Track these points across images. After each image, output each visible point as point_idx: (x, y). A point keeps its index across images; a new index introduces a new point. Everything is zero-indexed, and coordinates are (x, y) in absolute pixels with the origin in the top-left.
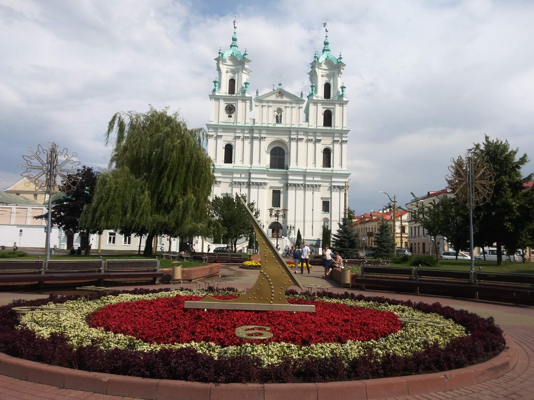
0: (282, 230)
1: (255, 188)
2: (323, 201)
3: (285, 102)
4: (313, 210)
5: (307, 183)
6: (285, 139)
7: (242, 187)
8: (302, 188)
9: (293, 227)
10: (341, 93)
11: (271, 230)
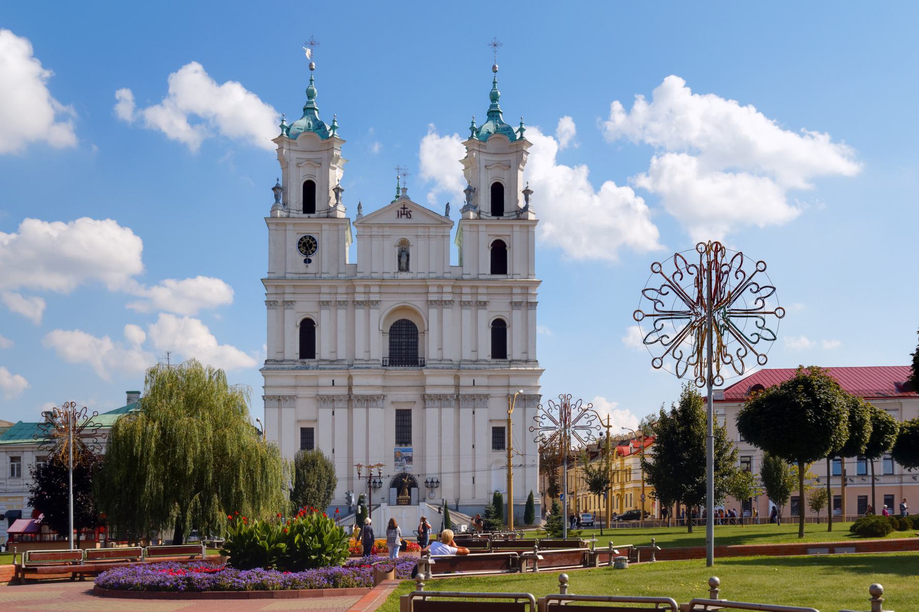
0: (416, 489)
1: (362, 407)
2: (494, 428)
3: (416, 226)
4: (473, 446)
6: (417, 302)
7: (336, 406)
8: (453, 402)
9: (437, 482)
10: (522, 204)
11: (395, 490)
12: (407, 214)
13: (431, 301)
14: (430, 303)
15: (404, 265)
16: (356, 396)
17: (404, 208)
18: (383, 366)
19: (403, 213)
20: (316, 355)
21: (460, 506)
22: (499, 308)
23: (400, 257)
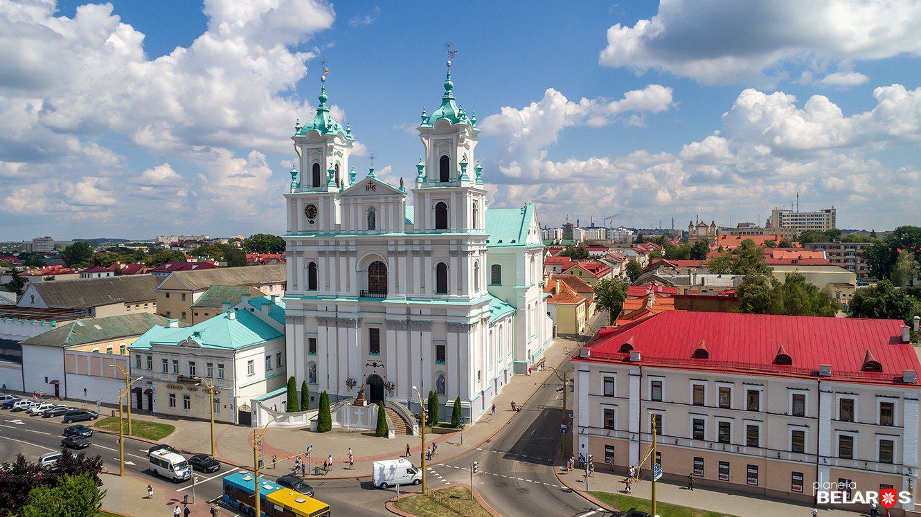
5: (413, 318)
13: (390, 252)
14: (391, 253)
16: (340, 319)
17: (371, 183)
22: (440, 255)
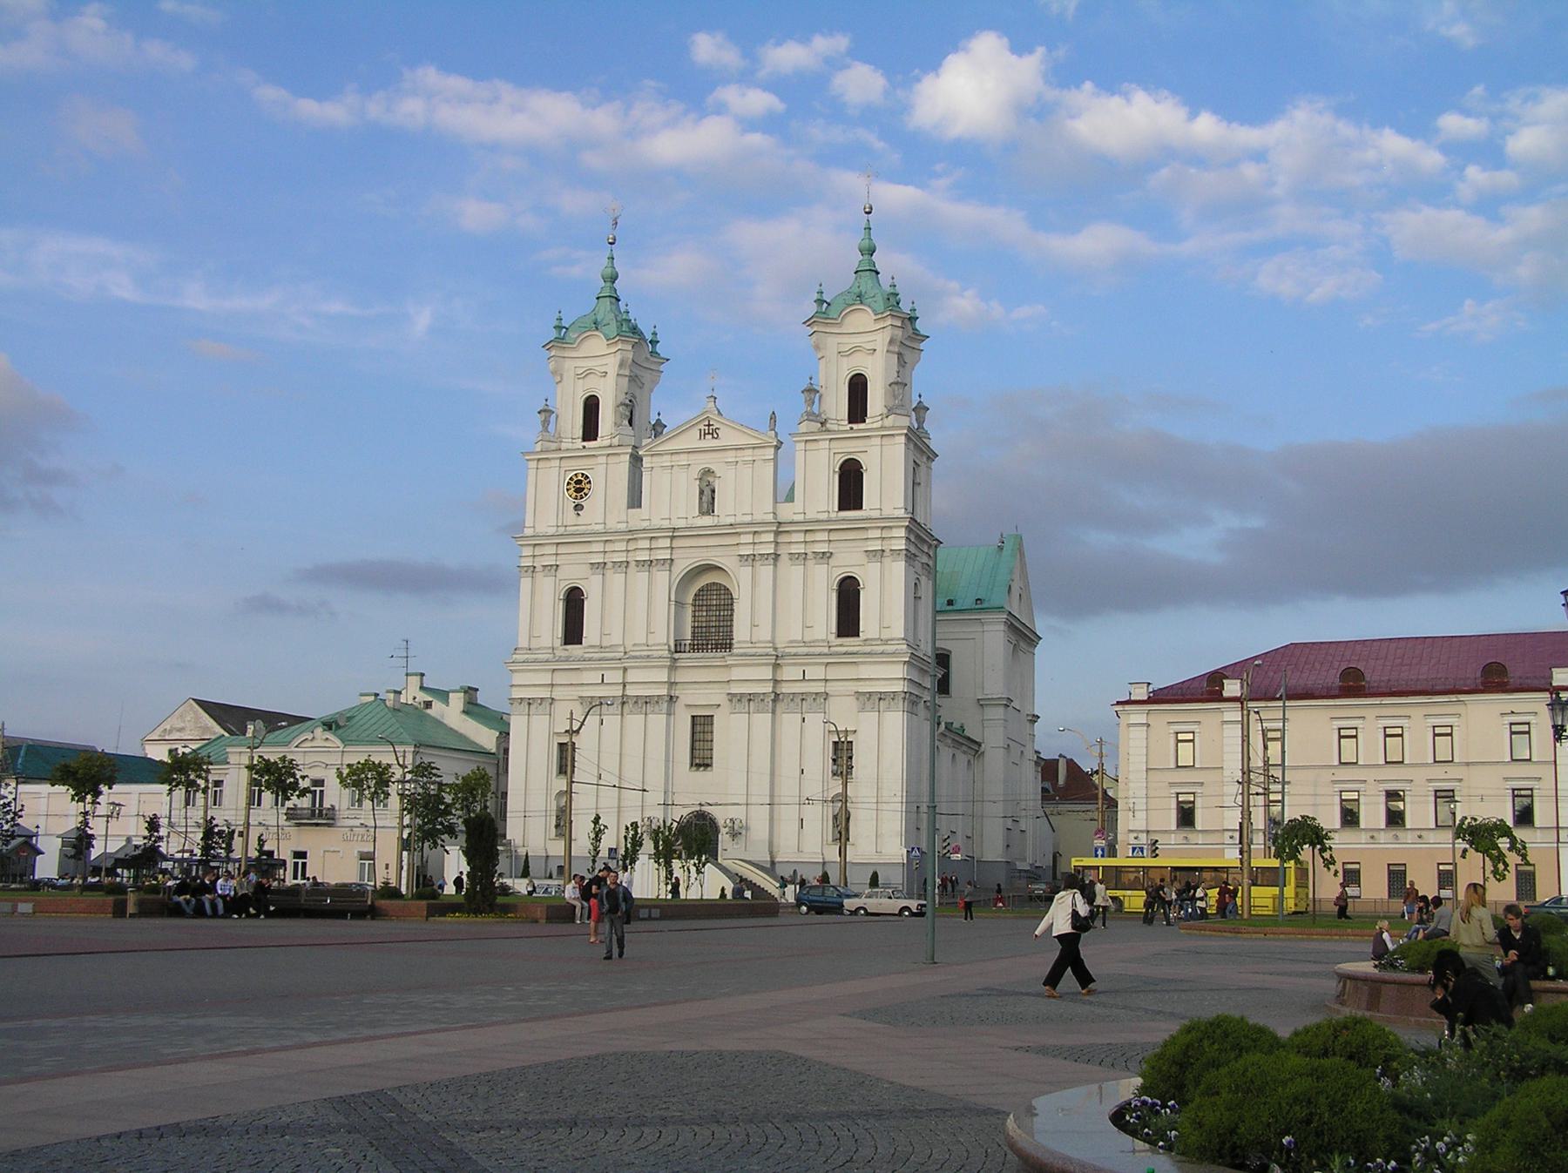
12: (712, 434)
15: (705, 505)
17: (709, 425)
18: (676, 652)
19: (707, 432)
20: (583, 639)
21: (779, 862)
23: (702, 492)
